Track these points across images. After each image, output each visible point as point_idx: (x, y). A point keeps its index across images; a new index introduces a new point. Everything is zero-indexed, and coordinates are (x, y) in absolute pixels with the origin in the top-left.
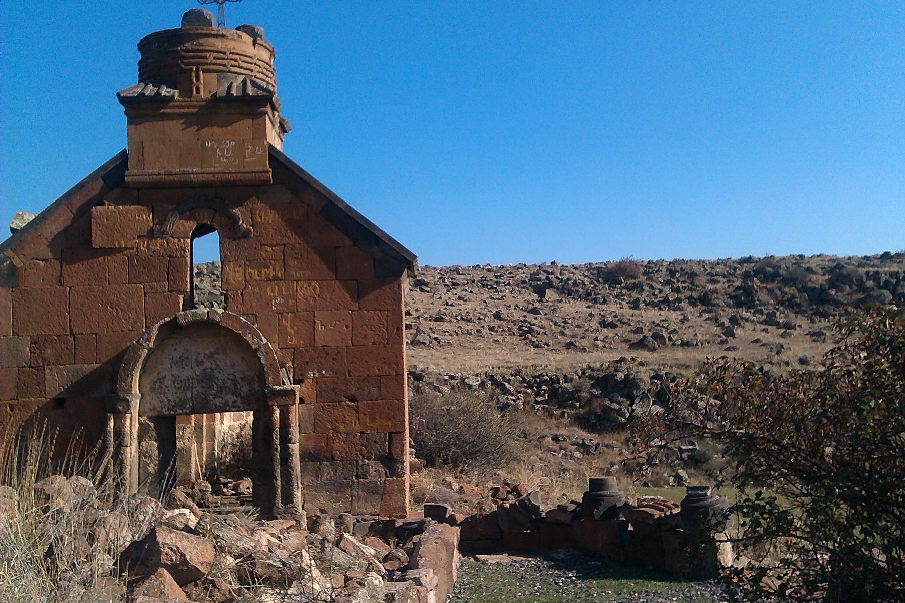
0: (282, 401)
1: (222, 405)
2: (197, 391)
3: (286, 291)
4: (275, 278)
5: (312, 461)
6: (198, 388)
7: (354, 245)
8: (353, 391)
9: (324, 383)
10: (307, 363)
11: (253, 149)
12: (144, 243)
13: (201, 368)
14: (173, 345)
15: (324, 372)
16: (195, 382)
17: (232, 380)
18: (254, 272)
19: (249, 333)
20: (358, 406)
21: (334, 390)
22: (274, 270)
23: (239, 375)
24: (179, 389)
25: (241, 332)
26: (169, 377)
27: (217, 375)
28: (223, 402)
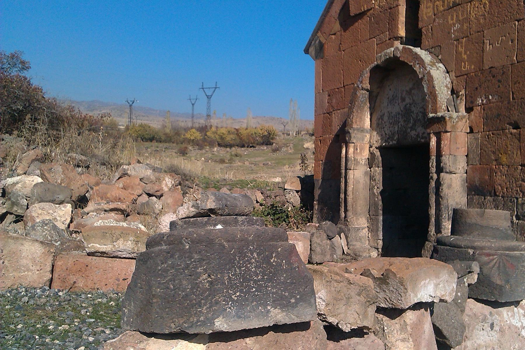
0: (436, 127)
1: (415, 136)
2: (401, 125)
3: (462, 15)
5: (478, 195)
8: (516, 116)
9: (490, 109)
10: (477, 88)
12: (452, 16)
14: (389, 86)
15: (490, 97)
16: (400, 117)
17: (422, 113)
19: (418, 64)
20: (520, 134)
21: (499, 115)
24: (391, 124)
25: (412, 64)
26: (386, 114)
27: (413, 109)
28: (417, 134)
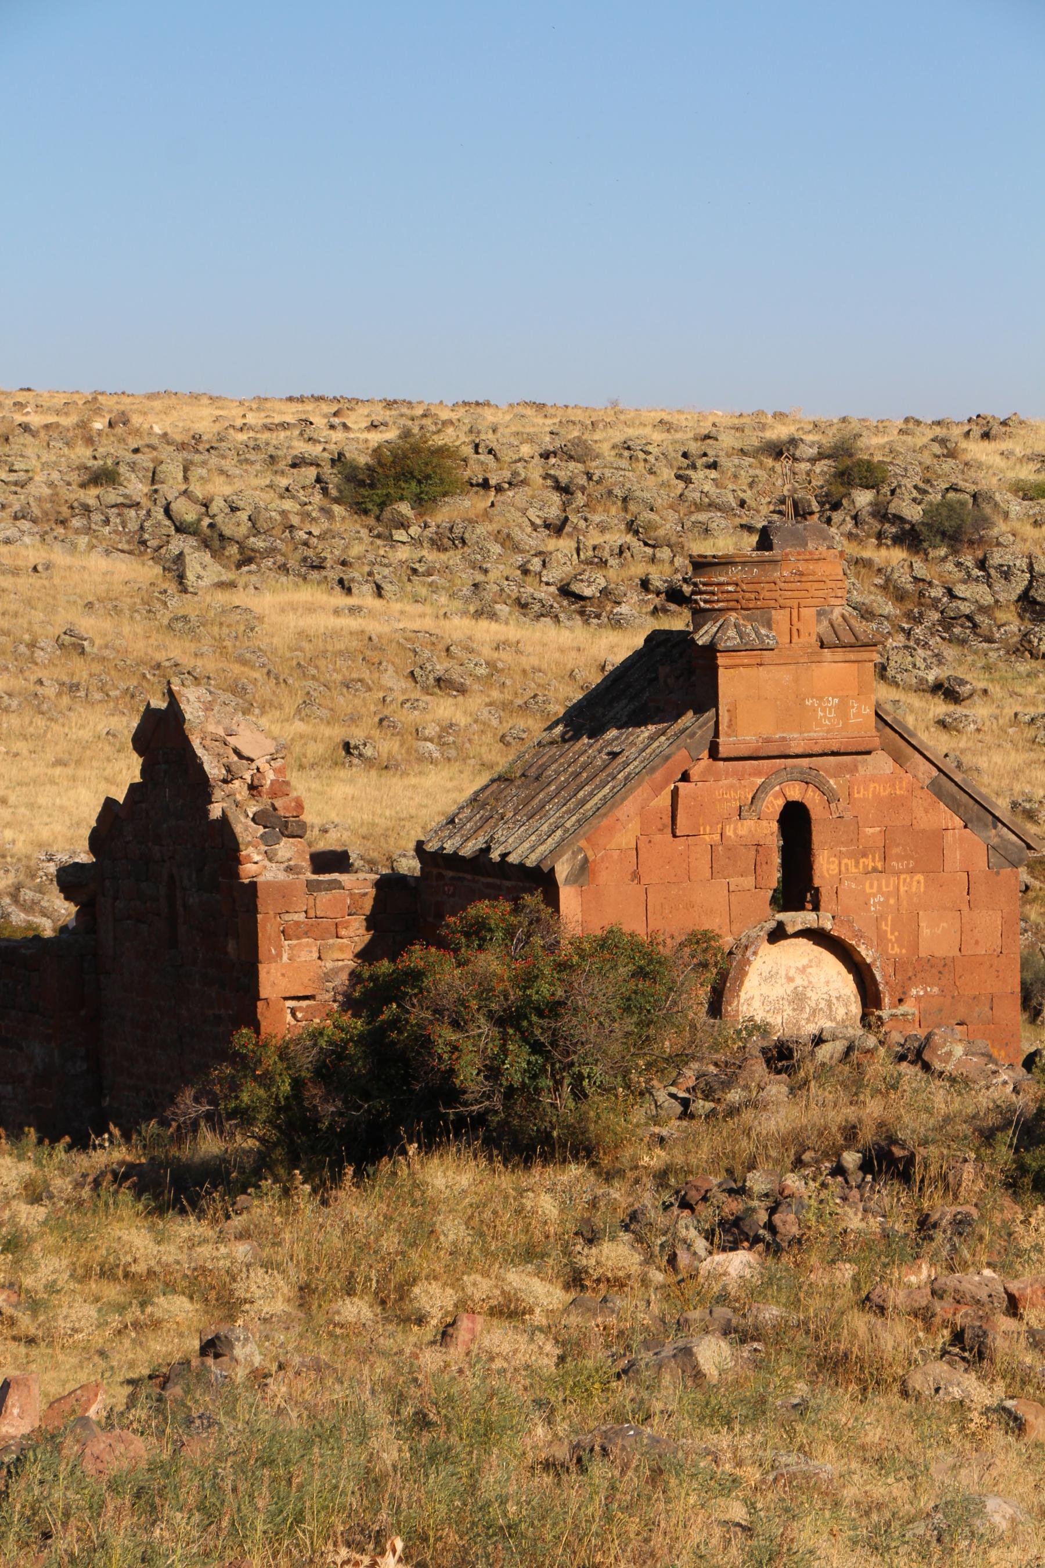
4: (875, 870)
6: (788, 1011)
7: (966, 827)
8: (962, 1012)
11: (859, 708)
13: (792, 985)
16: (786, 1003)
18: (851, 863)
22: (873, 860)
23: (834, 994)
27: (809, 994)
